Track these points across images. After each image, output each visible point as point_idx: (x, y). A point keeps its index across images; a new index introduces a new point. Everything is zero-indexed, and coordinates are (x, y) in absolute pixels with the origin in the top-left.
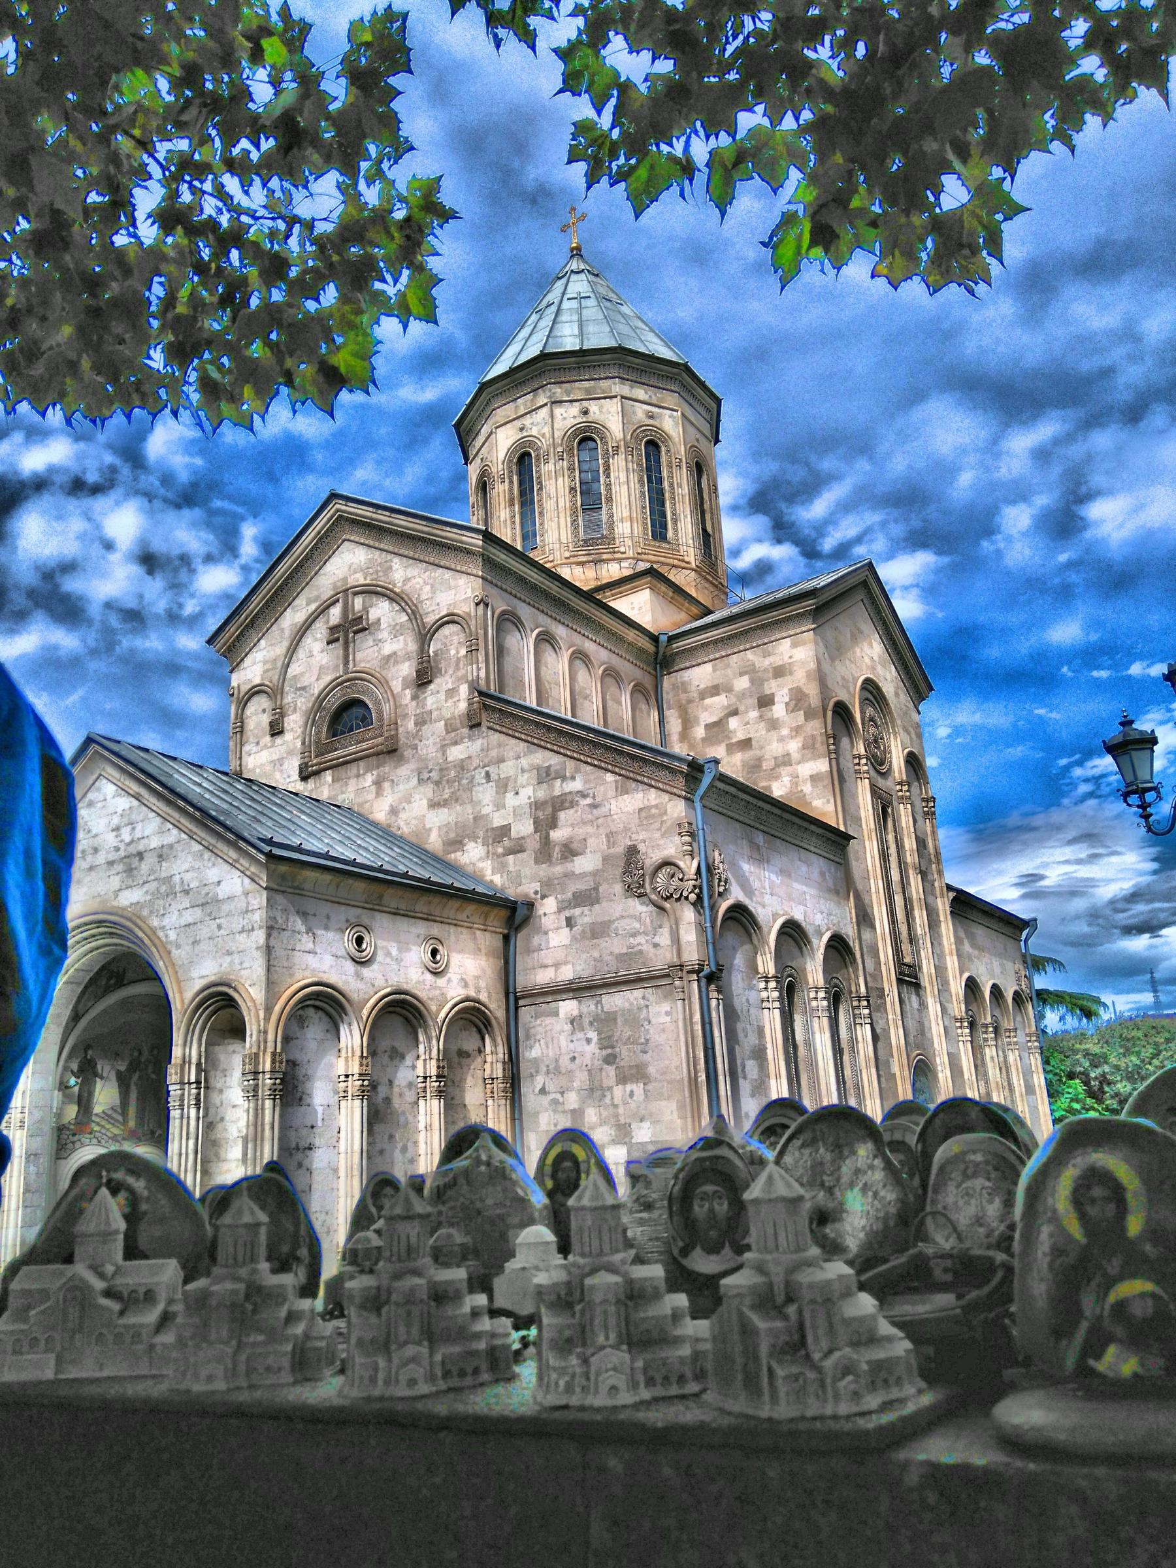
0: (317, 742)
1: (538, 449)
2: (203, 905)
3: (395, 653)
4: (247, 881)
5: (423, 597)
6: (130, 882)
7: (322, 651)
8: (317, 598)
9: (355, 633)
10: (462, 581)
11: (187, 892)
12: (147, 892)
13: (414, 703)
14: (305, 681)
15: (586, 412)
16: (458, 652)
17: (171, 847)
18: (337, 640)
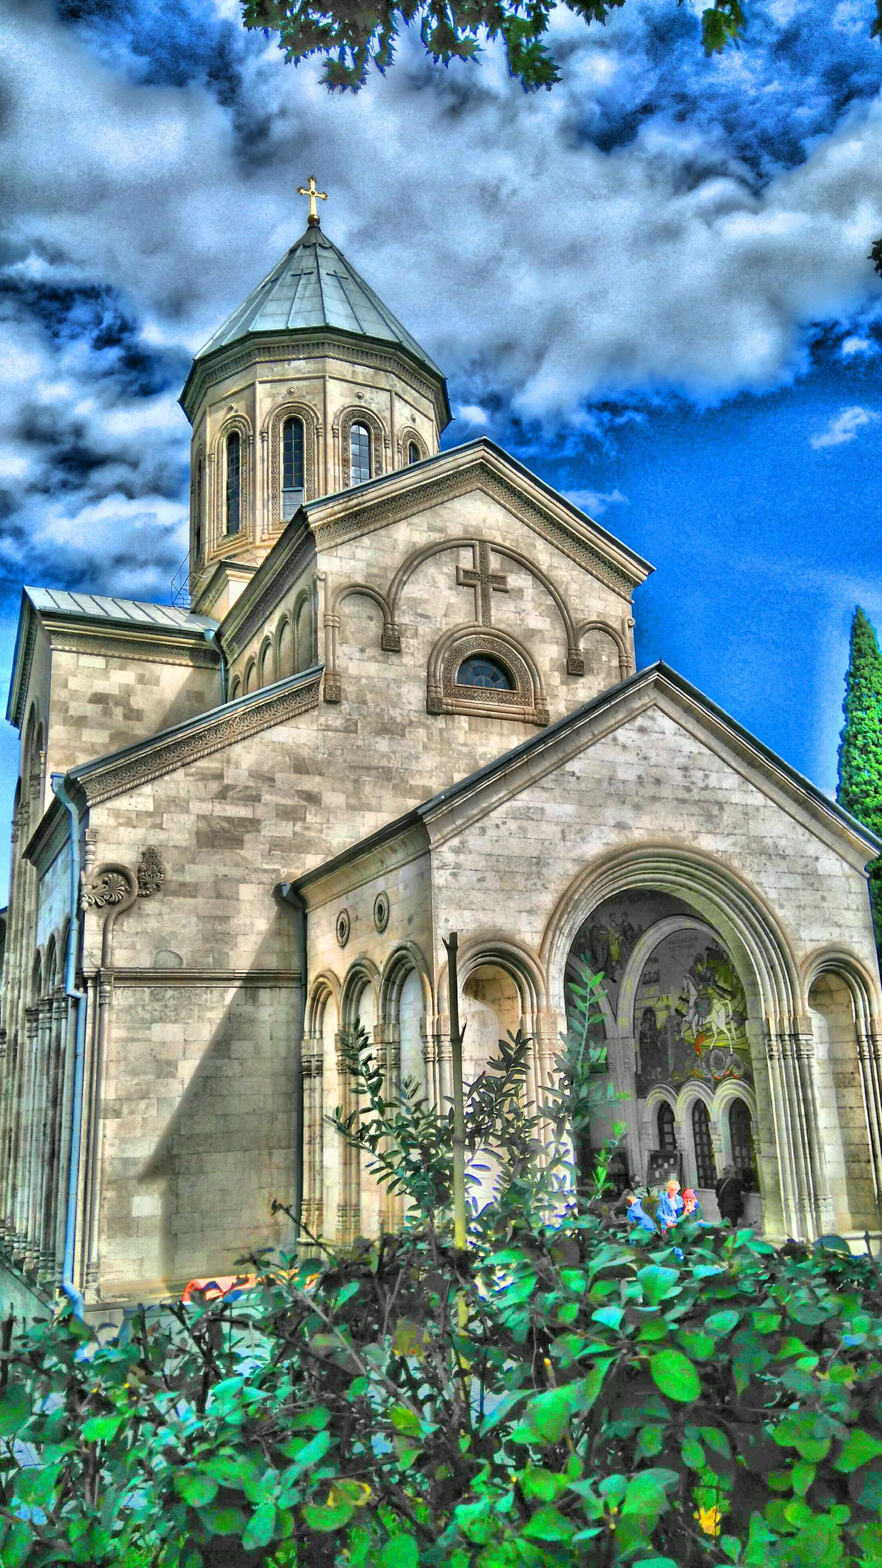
0: (447, 680)
1: (378, 428)
2: (803, 874)
3: (541, 631)
4: (846, 866)
5: (571, 592)
6: (710, 827)
7: (450, 588)
8: (442, 530)
9: (495, 589)
10: (613, 597)
11: (784, 857)
12: (735, 844)
13: (564, 688)
14: (430, 611)
15: (414, 420)
16: (609, 661)
17: (758, 809)
18: (474, 586)
